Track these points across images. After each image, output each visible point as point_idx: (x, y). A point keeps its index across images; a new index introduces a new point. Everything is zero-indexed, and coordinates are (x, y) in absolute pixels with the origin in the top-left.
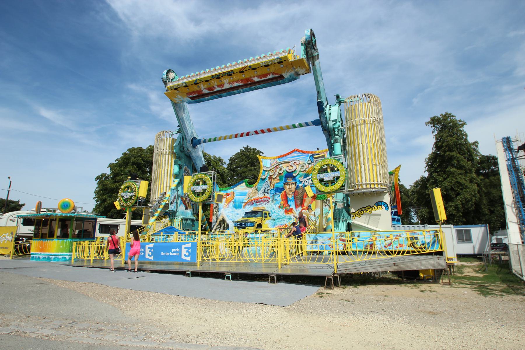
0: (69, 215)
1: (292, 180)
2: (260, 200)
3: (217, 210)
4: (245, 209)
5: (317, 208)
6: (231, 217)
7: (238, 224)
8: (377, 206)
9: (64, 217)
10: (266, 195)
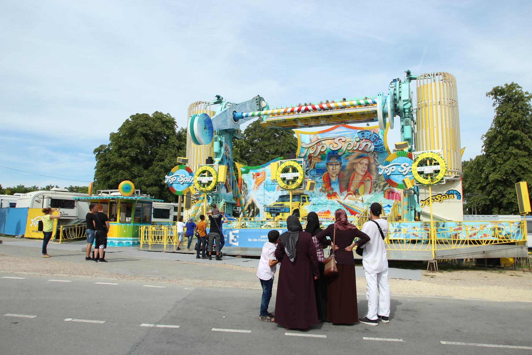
0: (130, 198)
1: (336, 160)
3: (246, 193)
5: (366, 193)
6: (262, 201)
7: (270, 209)
8: (448, 195)
9: (125, 200)
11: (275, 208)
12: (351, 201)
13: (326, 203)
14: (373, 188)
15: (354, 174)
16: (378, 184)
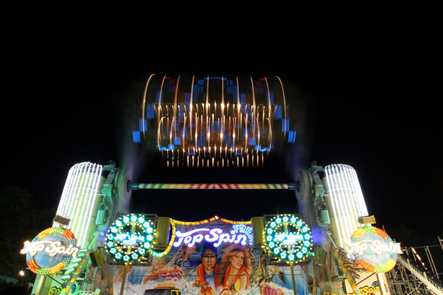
1: (212, 252)
2: (169, 274)
4: (145, 285)
5: (242, 289)
10: (178, 268)
14: (250, 283)
15: (230, 268)
16: (253, 279)
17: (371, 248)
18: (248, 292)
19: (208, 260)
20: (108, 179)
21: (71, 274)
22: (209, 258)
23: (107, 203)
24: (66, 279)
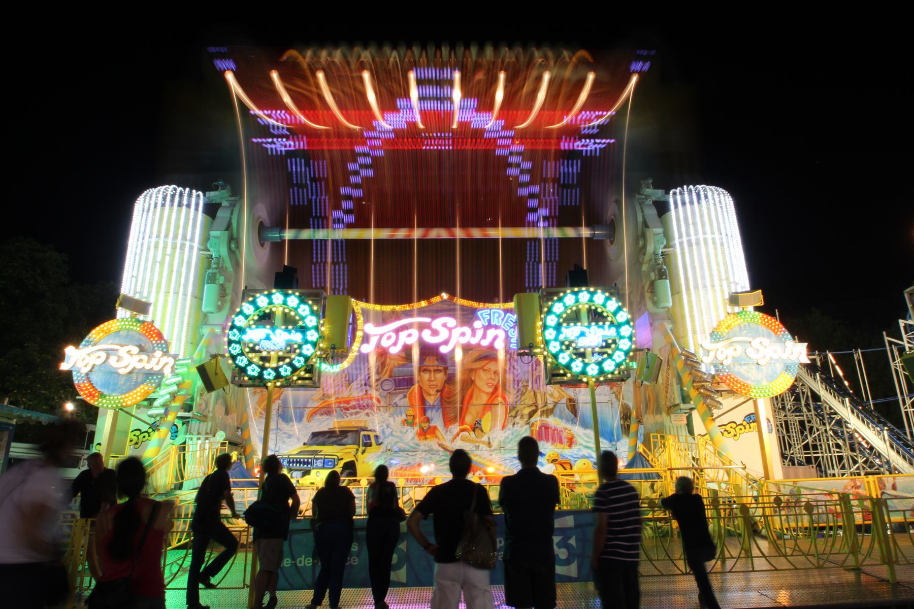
1: (436, 363)
4: (311, 424)
11: (300, 459)
12: (468, 444)
13: (415, 448)
14: (510, 419)
16: (517, 412)
17: (750, 352)
18: (506, 434)
19: (430, 378)
20: (217, 220)
21: (166, 406)
22: (430, 374)
23: (221, 269)
24: (157, 415)
